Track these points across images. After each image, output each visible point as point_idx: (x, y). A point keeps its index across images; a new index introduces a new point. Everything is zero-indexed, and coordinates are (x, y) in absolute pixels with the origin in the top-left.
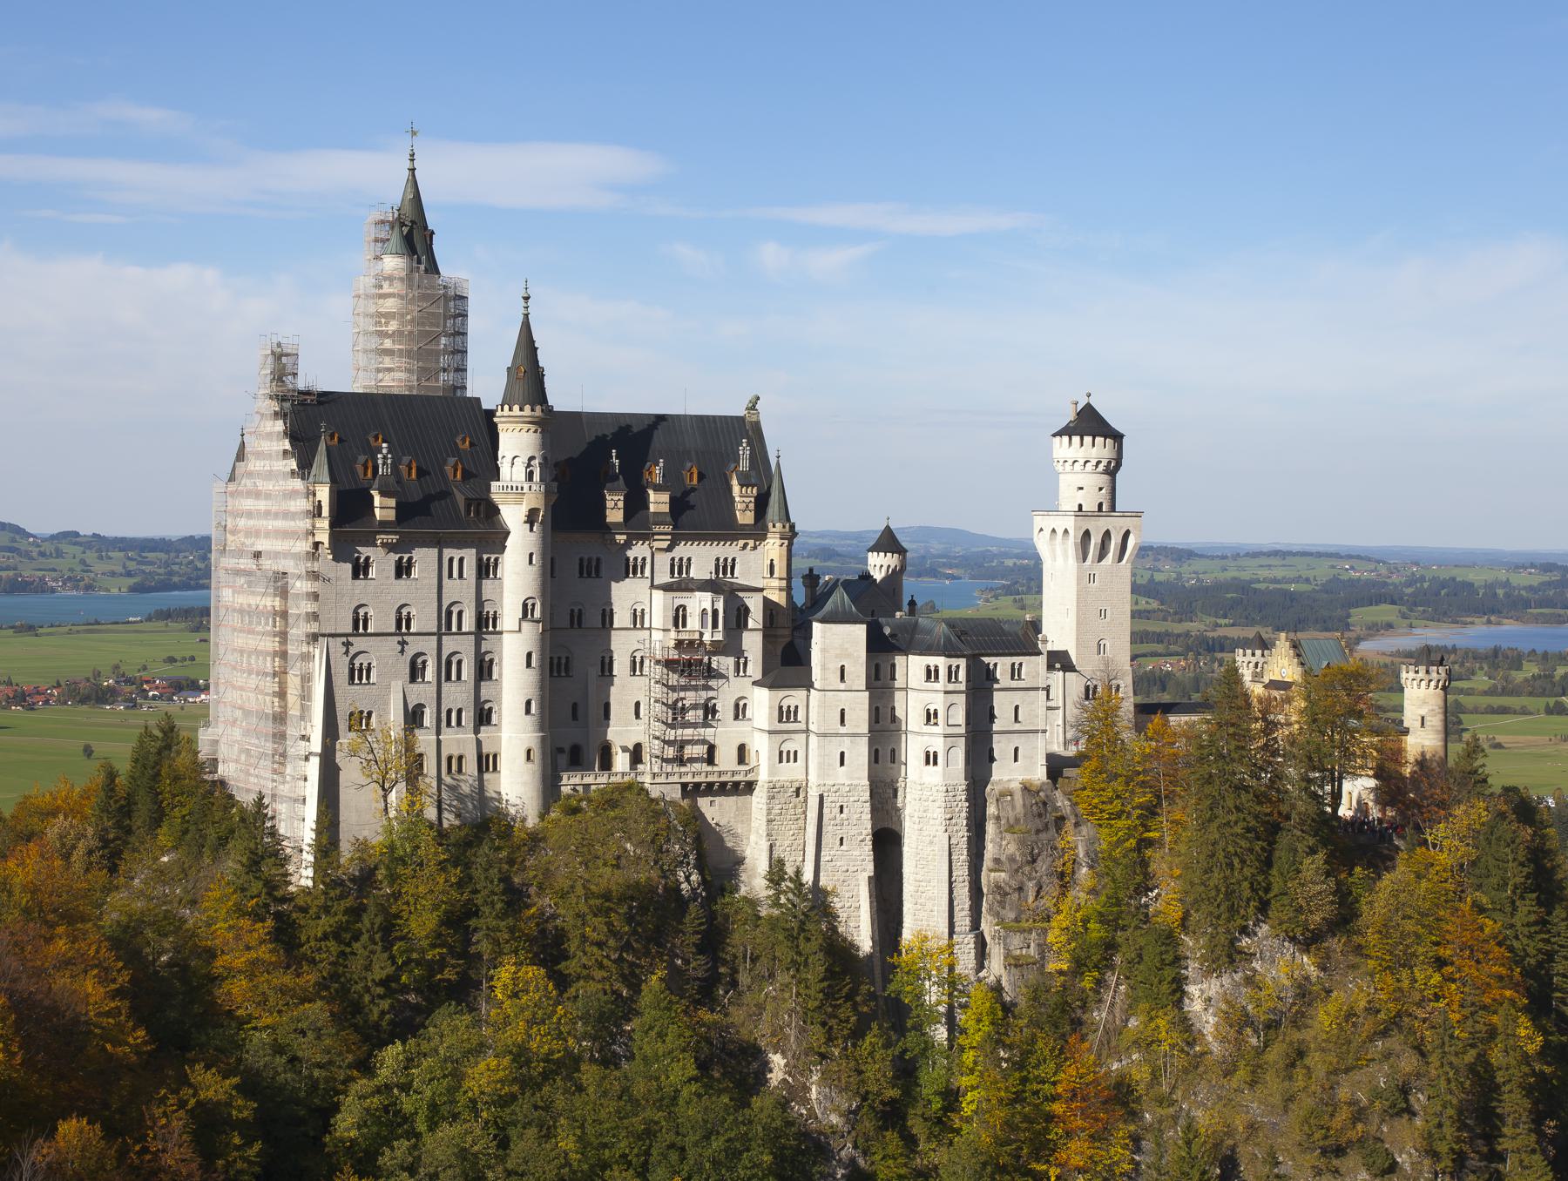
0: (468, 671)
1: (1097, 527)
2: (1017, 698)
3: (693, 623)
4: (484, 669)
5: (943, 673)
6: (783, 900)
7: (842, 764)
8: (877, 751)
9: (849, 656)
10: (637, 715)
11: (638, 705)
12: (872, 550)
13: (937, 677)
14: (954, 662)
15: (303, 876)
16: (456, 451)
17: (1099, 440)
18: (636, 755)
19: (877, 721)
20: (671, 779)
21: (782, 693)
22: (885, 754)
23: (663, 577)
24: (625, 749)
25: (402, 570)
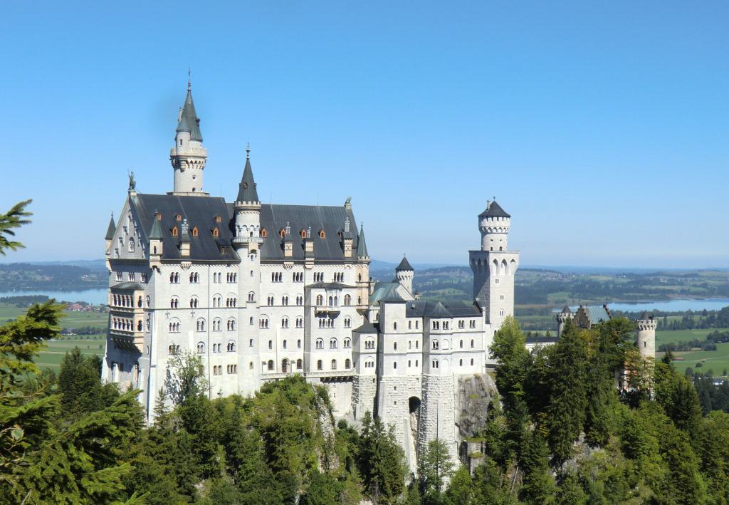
0: (224, 325)
1: (500, 258)
2: (472, 336)
3: (326, 302)
4: (231, 325)
5: (441, 325)
6: (370, 431)
7: (395, 367)
8: (410, 362)
9: (398, 318)
10: (299, 346)
11: (299, 341)
12: (398, 269)
13: (438, 327)
14: (446, 320)
15: (150, 421)
16: (215, 224)
17: (500, 218)
18: (299, 366)
19: (410, 348)
20: (316, 376)
21: (366, 335)
22: (413, 363)
23: (309, 280)
24: (293, 362)
25: (194, 278)
